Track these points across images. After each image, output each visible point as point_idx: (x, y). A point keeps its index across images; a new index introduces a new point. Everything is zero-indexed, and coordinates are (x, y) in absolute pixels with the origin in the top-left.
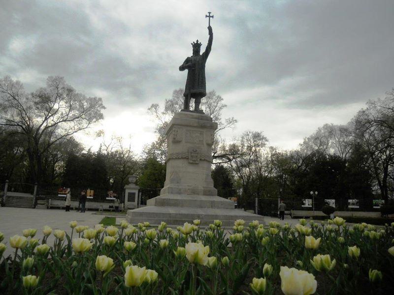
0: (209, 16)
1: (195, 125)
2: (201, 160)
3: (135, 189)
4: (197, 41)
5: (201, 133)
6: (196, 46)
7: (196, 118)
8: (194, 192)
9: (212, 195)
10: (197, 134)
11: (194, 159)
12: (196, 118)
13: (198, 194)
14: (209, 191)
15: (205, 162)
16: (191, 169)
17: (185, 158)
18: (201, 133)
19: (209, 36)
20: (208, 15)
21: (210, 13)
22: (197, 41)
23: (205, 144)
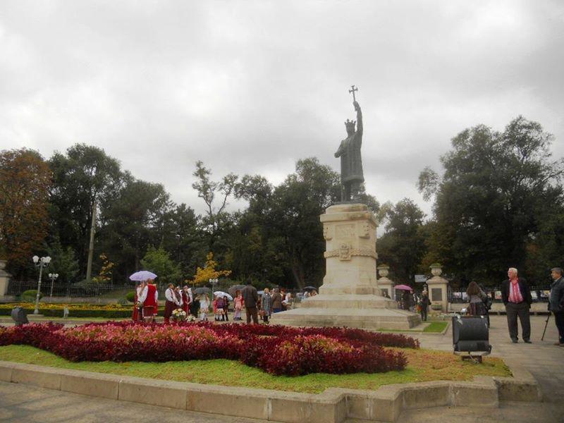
0: (353, 90)
1: (344, 219)
2: (352, 256)
3: (440, 283)
4: (348, 120)
5: (353, 226)
6: (350, 126)
7: (345, 211)
8: (346, 292)
9: (367, 294)
10: (348, 228)
11: (344, 256)
12: (345, 211)
13: (350, 293)
14: (363, 289)
15: (358, 258)
16: (344, 266)
17: (336, 256)
18: (353, 226)
19: (356, 113)
20: (355, 88)
21: (353, 87)
22: (348, 120)
23: (357, 236)
